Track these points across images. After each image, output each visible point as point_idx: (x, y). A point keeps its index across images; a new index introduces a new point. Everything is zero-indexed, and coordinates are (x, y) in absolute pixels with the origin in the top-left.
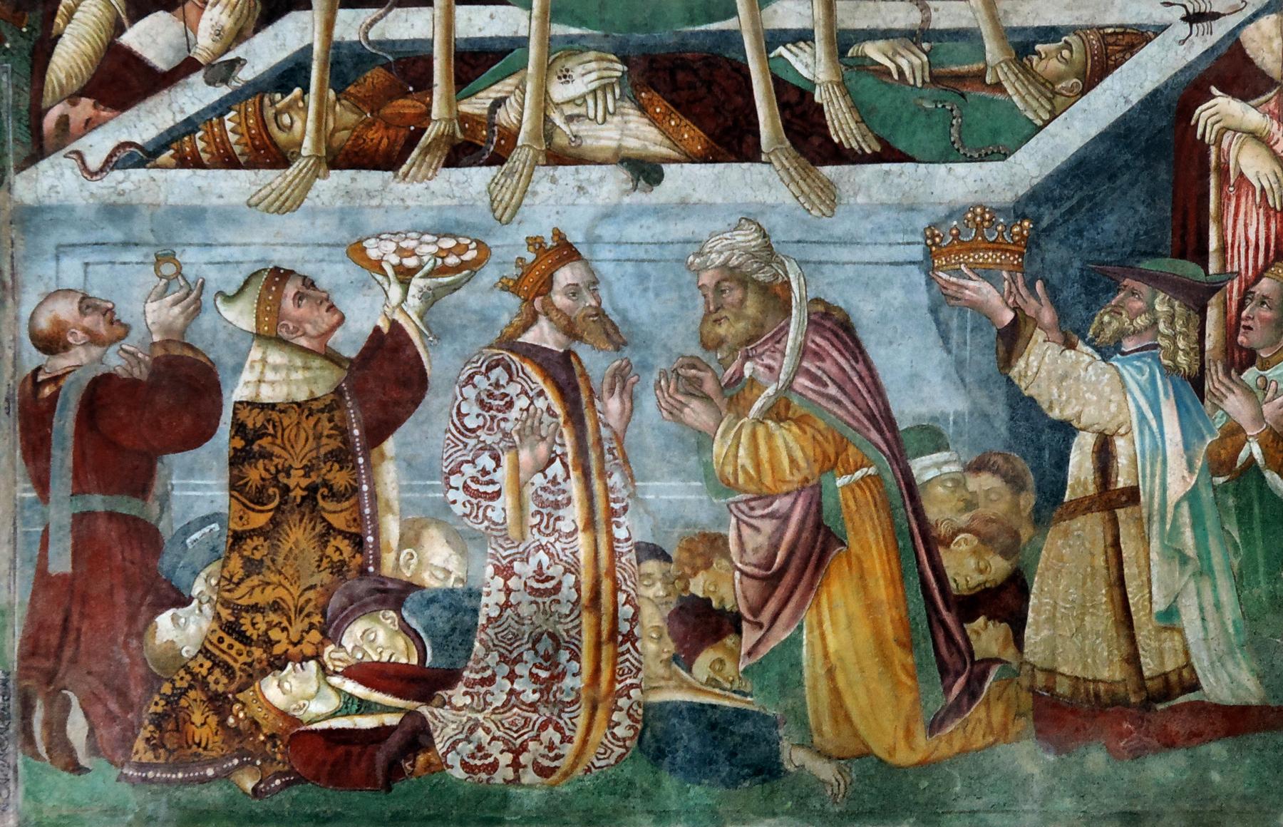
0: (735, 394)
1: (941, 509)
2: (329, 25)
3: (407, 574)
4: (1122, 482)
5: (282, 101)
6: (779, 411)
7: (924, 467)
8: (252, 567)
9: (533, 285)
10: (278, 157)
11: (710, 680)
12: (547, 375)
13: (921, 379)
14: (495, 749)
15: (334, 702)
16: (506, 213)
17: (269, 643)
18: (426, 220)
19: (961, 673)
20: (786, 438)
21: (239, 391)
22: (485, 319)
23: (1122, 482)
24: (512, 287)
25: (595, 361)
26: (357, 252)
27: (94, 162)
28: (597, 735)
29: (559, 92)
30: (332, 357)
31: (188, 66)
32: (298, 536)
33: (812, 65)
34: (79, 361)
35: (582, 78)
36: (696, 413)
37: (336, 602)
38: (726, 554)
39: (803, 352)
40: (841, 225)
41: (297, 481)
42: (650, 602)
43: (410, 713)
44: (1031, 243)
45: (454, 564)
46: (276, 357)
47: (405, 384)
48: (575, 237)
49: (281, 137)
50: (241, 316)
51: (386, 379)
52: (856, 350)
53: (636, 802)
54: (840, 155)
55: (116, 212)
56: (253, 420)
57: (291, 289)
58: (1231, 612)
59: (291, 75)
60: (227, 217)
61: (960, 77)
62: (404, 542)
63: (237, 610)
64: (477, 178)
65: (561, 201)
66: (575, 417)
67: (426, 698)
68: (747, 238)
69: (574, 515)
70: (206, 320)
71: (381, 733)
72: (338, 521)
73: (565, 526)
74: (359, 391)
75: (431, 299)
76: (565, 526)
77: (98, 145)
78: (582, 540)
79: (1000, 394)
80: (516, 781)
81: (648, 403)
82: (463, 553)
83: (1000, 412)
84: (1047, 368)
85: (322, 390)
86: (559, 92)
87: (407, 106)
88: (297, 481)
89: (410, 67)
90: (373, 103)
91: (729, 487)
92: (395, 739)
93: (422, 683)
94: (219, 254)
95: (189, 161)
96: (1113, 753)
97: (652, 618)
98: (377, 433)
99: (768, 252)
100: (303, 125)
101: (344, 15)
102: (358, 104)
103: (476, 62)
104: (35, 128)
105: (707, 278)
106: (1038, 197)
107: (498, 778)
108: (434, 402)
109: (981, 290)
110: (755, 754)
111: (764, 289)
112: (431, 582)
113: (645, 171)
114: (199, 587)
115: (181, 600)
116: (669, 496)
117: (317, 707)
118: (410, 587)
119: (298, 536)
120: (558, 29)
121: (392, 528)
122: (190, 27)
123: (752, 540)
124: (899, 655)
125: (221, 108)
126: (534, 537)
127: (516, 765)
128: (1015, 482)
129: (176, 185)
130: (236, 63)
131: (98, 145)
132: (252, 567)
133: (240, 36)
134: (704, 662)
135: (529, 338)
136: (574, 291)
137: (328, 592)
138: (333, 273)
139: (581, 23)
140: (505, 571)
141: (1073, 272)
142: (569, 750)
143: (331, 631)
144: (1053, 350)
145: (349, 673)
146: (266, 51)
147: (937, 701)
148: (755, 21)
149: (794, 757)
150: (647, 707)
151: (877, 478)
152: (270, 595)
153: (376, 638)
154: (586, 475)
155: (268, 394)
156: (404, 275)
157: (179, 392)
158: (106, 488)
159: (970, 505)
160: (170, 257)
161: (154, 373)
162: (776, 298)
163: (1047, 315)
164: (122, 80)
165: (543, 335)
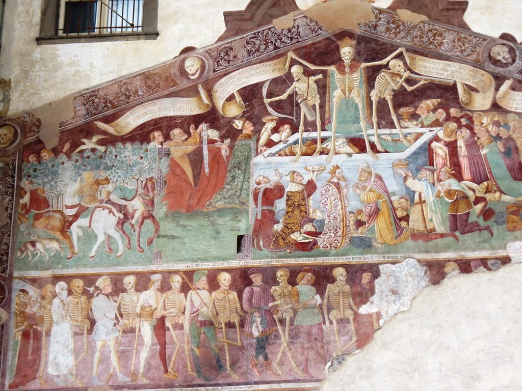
0: (364, 188)
1: (396, 205)
2: (302, 135)
3: (314, 217)
4: (423, 199)
5: (294, 146)
6: (371, 191)
7: (393, 198)
8: (289, 217)
9: (333, 172)
10: (294, 154)
11: (361, 232)
12: (335, 185)
13: (392, 185)
14: (327, 244)
15: (302, 238)
16: (329, 162)
17: (292, 229)
18: (316, 163)
19: (400, 229)
20: (372, 194)
21: (287, 190)
22: (325, 178)
23: (423, 199)
24: (330, 173)
25: (342, 184)
26: (306, 168)
27: (266, 156)
28: (344, 241)
29: (336, 144)
30: (302, 184)
31: (281, 141)
32: (297, 212)
33: (374, 139)
34: (263, 187)
35: (340, 141)
36: (358, 191)
37: (302, 222)
38: (363, 212)
39: (374, 181)
40: (379, 162)
41: (296, 203)
42: (351, 221)
43: (314, 239)
44: (408, 164)
45: (321, 215)
46: (293, 184)
47: (313, 188)
48: (339, 165)
49: (294, 151)
50: (288, 178)
51: (311, 187)
52: (382, 181)
53: (350, 252)
54: (378, 152)
55: (268, 163)
56: (290, 194)
57: (296, 174)
58: (440, 219)
59: (296, 142)
60: (286, 163)
61: (396, 140)
62: (313, 212)
63: (287, 224)
64: (324, 157)
65: (336, 160)
66: (339, 192)
67: (317, 237)
68: (365, 165)
69: (339, 207)
70: (283, 179)
71: (310, 242)
72: (303, 209)
73: (338, 209)
74: (306, 189)
75: (317, 175)
76: (338, 209)
77: (266, 153)
78: (341, 211)
79: (404, 187)
80: (331, 249)
81: (351, 190)
82: (322, 214)
83: (404, 190)
84: (411, 183)
85: (301, 189)
86: (336, 144)
87: (313, 146)
88: (296, 203)
89: (314, 141)
90: (309, 146)
91: (364, 202)
92: (311, 244)
93: (316, 234)
94: (284, 169)
95: (279, 155)
96: (424, 242)
97: (352, 223)
98: (309, 196)
99: (368, 167)
100: (298, 149)
101: (304, 133)
102: (306, 146)
103: (323, 140)
104: (257, 151)
105: (360, 171)
106: (409, 157)
107: (328, 249)
108: (317, 191)
109: (401, 171)
110: (368, 244)
111: (368, 172)
112: (317, 218)
113: (350, 155)
114: (281, 220)
115: (278, 223)
116: (354, 204)
117: (299, 239)
118: (314, 219)
119: (297, 212)
120: (336, 135)
121: (311, 210)
122: (281, 136)
123: (367, 210)
124: (390, 227)
125: (285, 147)
126: (333, 211)
127: (331, 247)
128: (407, 200)
129: (278, 159)
130: (287, 141)
131: (266, 153)
132: (289, 217)
133: (288, 137)
134: (360, 229)
135: (332, 180)
136: (339, 173)
137: (301, 221)
138: (302, 172)
139: (340, 133)
140: (329, 216)
141: (414, 168)
142: (339, 244)
143: (302, 227)
144: (412, 180)
145: (304, 233)
146: (292, 139)
147: (396, 234)
148: (366, 133)
149: (374, 244)
150: (351, 237)
151: (386, 200)
152: (292, 221)
153: (309, 227)
154: (341, 201)
155: (292, 190)
156: (313, 171)
157: (279, 190)
158: (267, 205)
159: (400, 204)
160: (277, 170)
161: (274, 187)
162: (370, 173)
163: (411, 175)
164: (270, 144)
165: (335, 180)
